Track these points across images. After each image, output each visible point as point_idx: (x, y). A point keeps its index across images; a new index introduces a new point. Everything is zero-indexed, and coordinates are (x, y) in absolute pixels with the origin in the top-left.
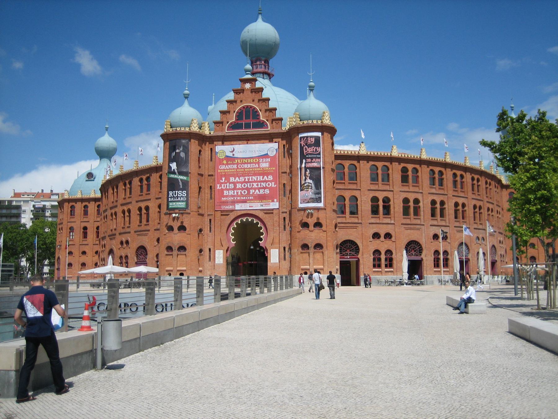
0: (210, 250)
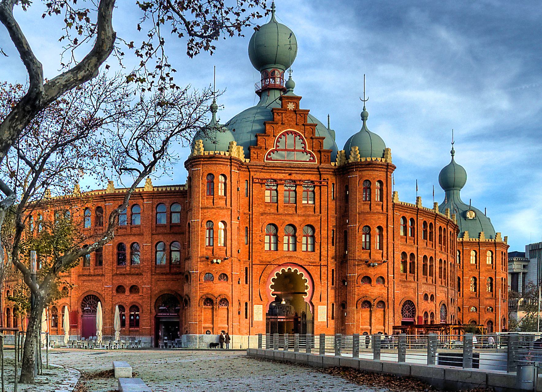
0: (246, 304)
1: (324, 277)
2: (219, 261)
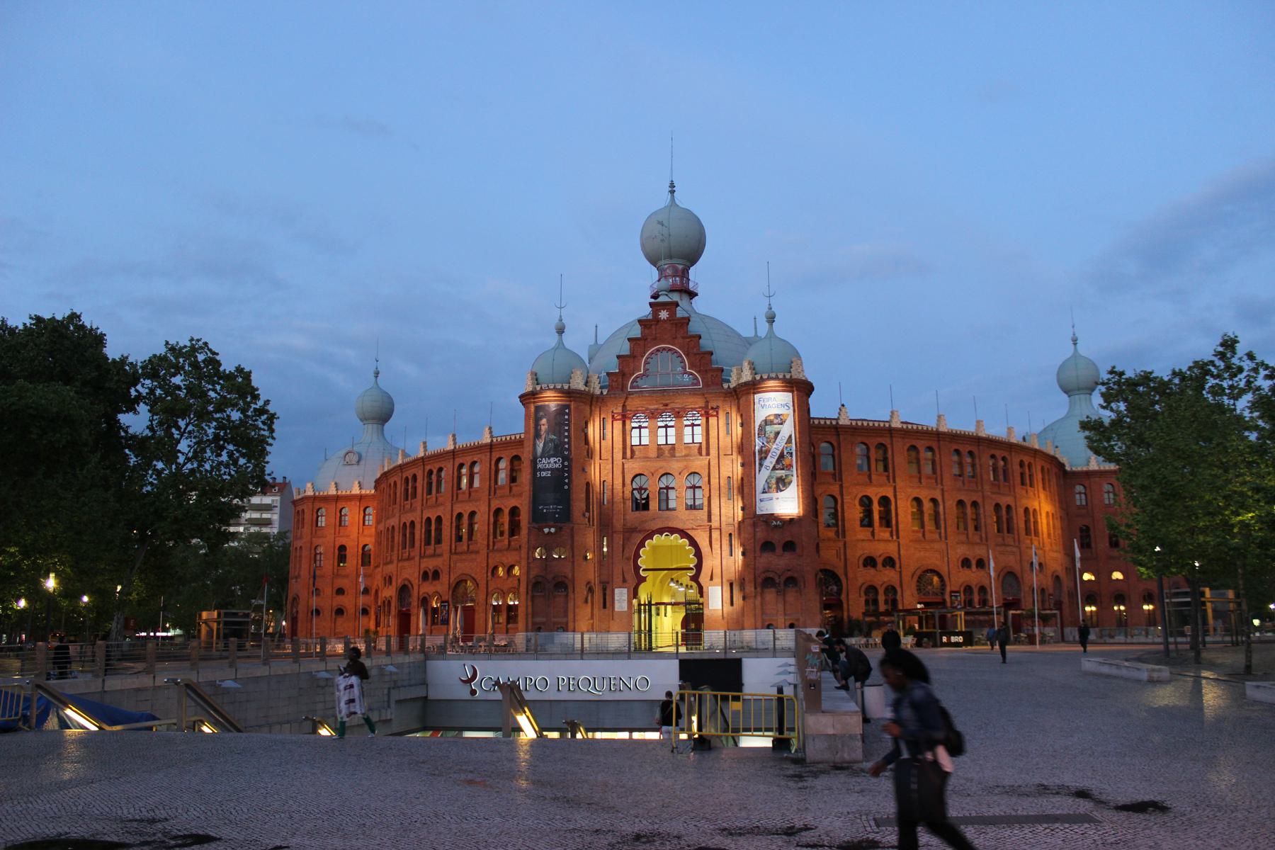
1: (716, 545)
2: (553, 530)
